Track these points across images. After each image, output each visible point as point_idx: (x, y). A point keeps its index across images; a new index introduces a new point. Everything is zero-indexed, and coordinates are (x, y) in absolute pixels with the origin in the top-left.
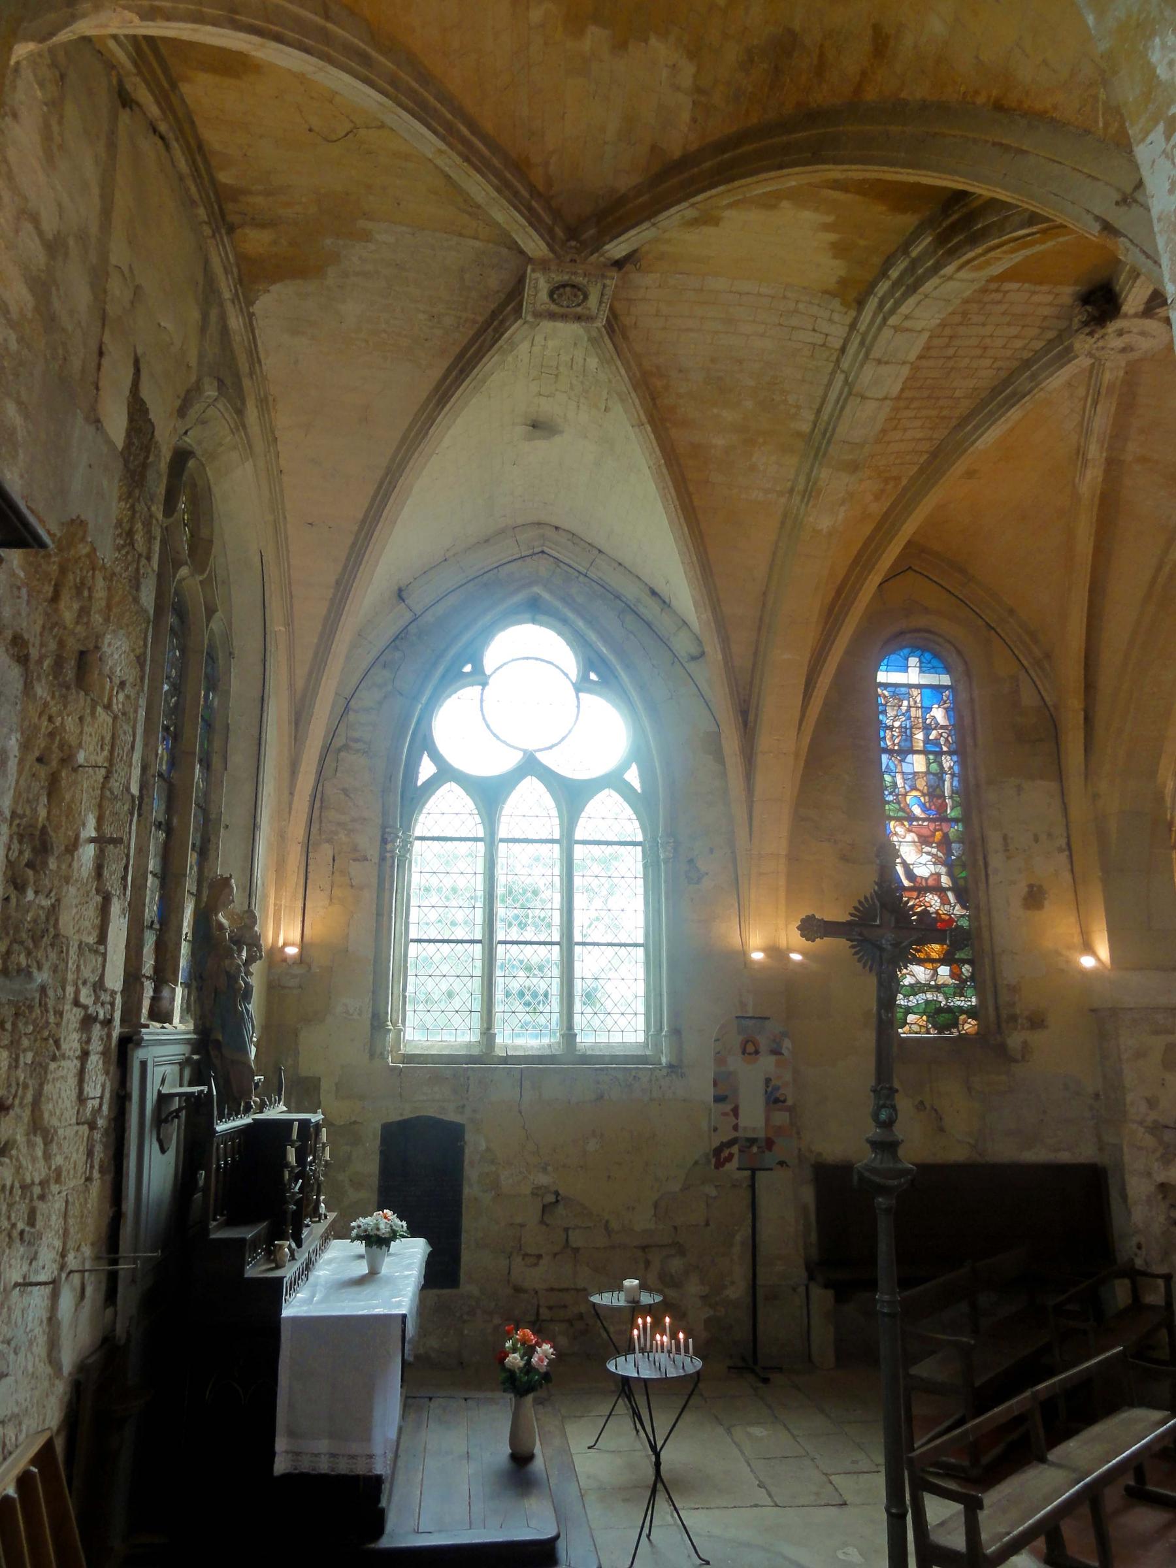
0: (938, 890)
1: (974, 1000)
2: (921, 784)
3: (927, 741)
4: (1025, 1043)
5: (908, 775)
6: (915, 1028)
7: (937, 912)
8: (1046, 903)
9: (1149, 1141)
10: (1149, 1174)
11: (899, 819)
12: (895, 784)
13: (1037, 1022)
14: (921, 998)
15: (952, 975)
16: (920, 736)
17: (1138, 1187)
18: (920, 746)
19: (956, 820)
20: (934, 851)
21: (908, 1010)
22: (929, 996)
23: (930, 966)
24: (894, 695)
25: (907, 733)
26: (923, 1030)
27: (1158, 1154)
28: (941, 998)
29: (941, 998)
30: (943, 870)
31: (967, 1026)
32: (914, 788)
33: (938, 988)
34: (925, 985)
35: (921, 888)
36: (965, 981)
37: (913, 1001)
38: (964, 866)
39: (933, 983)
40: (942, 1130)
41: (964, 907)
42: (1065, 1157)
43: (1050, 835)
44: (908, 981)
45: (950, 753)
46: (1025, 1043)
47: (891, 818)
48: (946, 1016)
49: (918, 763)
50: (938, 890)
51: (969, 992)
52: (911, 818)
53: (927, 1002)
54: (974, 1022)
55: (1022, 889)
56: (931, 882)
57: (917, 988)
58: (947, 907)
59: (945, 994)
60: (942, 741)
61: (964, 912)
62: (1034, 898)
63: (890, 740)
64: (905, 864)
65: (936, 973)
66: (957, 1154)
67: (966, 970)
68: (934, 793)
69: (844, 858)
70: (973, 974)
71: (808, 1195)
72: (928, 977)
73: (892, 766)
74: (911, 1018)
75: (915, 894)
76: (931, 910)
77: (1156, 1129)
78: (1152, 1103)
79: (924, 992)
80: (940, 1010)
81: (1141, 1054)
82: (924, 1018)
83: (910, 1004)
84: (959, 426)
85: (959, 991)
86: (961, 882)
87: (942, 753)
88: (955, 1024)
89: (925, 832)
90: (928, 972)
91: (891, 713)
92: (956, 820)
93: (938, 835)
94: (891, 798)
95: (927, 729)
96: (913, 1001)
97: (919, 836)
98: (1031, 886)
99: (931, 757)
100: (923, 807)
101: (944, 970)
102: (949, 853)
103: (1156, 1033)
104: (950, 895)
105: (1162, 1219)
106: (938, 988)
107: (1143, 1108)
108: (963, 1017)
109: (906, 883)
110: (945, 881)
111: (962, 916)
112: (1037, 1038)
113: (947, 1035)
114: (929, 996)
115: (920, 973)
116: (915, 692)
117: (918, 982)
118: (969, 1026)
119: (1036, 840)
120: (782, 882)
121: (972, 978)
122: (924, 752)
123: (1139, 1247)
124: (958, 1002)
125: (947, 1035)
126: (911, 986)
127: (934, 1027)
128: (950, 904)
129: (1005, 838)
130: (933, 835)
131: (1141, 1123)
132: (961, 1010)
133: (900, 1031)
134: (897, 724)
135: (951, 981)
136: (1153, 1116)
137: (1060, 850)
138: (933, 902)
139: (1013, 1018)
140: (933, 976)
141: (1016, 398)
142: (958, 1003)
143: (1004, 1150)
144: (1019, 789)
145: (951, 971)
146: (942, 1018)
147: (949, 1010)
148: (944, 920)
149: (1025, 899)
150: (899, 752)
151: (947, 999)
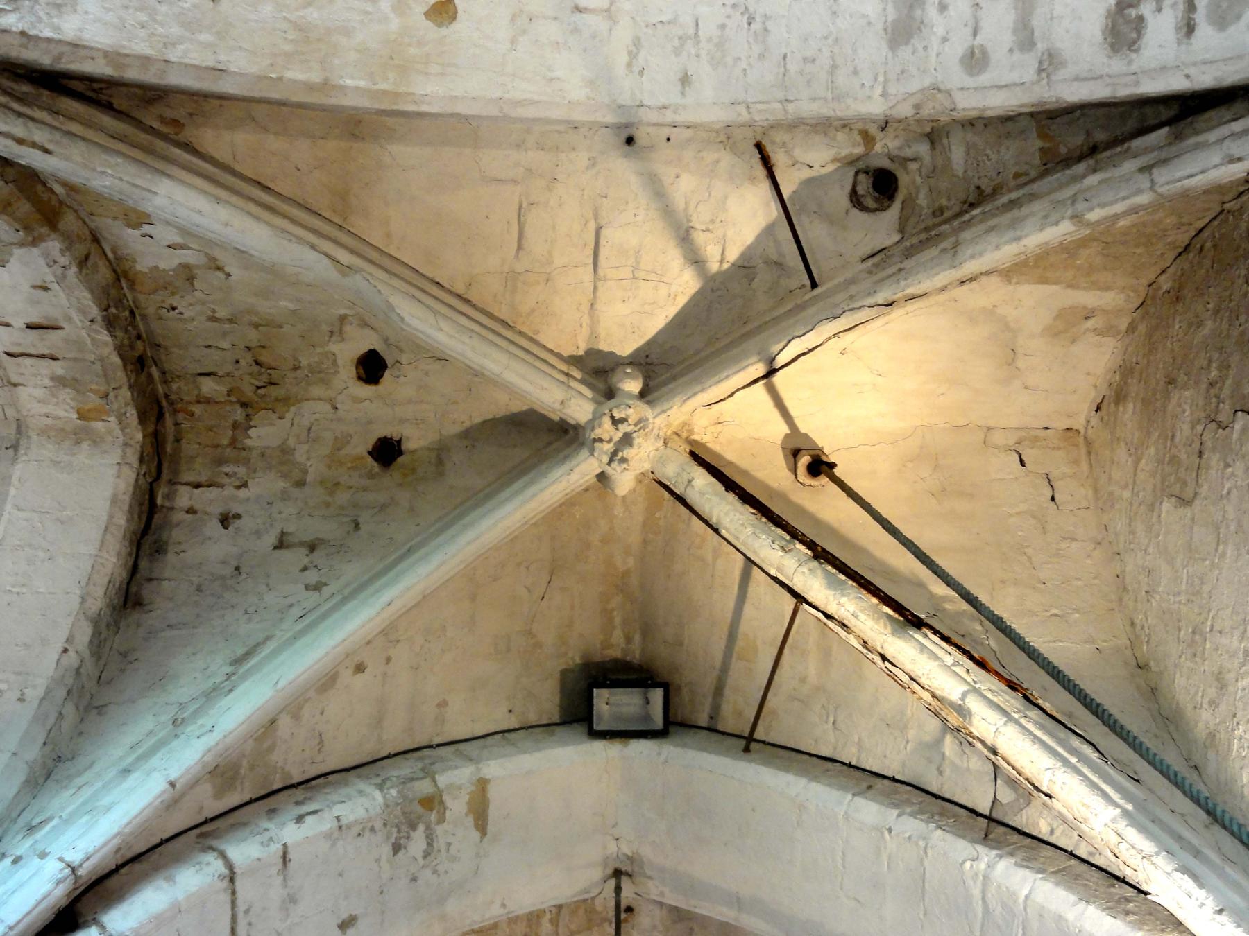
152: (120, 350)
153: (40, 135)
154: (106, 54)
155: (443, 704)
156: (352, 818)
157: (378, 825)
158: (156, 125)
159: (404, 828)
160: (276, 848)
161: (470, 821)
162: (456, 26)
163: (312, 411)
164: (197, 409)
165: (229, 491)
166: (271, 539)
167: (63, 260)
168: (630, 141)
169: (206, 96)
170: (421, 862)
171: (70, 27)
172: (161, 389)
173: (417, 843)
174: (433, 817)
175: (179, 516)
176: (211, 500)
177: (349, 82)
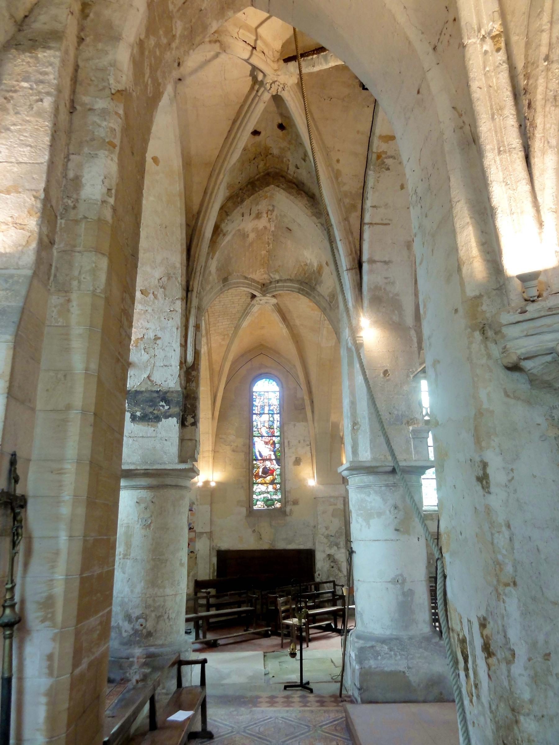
0: (270, 460)
2: (266, 425)
3: (269, 410)
4: (291, 510)
5: (261, 422)
6: (260, 506)
8: (301, 463)
9: (325, 541)
10: (324, 551)
11: (258, 437)
12: (257, 425)
13: (295, 503)
14: (262, 496)
15: (273, 488)
16: (266, 409)
17: (320, 557)
18: (266, 411)
19: (278, 436)
20: (270, 447)
21: (257, 500)
22: (265, 495)
23: (265, 485)
24: (260, 395)
25: (263, 408)
27: (328, 545)
28: (269, 496)
30: (272, 453)
32: (264, 426)
33: (268, 493)
35: (264, 460)
37: (259, 497)
38: (279, 451)
40: (261, 539)
41: (279, 465)
42: (302, 547)
43: (304, 440)
44: (258, 491)
45: (277, 414)
46: (291, 510)
47: (255, 436)
49: (265, 418)
50: (270, 460)
51: (279, 494)
52: (262, 436)
55: (293, 459)
56: (268, 457)
57: (261, 493)
60: (275, 410)
62: (298, 462)
63: (256, 410)
64: (259, 452)
66: (266, 547)
67: (278, 486)
68: (271, 428)
69: (234, 451)
71: (215, 560)
73: (257, 419)
74: (258, 503)
75: (262, 461)
77: (327, 537)
78: (327, 528)
80: (268, 500)
81: (324, 512)
84: (239, 320)
86: (278, 457)
87: (274, 414)
89: (267, 440)
91: (257, 400)
92: (278, 436)
93: (271, 441)
94: (256, 430)
95: (269, 406)
96: (259, 497)
97: (265, 442)
98: (296, 458)
99: (270, 415)
100: (268, 433)
102: (275, 447)
103: (331, 505)
104: (274, 462)
105: (328, 566)
106: (268, 493)
107: (324, 530)
109: (259, 458)
110: (273, 457)
112: (295, 508)
113: (270, 508)
115: (263, 488)
116: (266, 393)
118: (278, 505)
119: (299, 442)
120: (211, 460)
121: (280, 489)
122: (269, 414)
123: (319, 575)
124: (275, 497)
125: (270, 508)
126: (259, 492)
127: (266, 505)
129: (289, 442)
130: (269, 442)
131: (322, 535)
132: (276, 500)
134: (259, 405)
136: (327, 532)
137: (307, 445)
139: (288, 502)
141: (248, 313)
143: (281, 545)
144: (295, 425)
146: (269, 502)
147: (272, 500)
149: (294, 462)
150: (259, 414)
152: (249, 197)
153: (199, 269)
154: (182, 256)
155: (358, 132)
156: (372, 184)
157: (378, 175)
158: (194, 222)
159: (383, 166)
160: (370, 209)
161: (390, 142)
162: (158, 157)
163: (270, 143)
164: (267, 165)
165: (290, 163)
166: (303, 162)
167: (226, 221)
168: (180, 80)
169: (186, 210)
170: (396, 160)
171: (178, 265)
172: (262, 174)
173: (389, 162)
174: (384, 156)
175: (295, 175)
176: (292, 169)
177: (178, 189)
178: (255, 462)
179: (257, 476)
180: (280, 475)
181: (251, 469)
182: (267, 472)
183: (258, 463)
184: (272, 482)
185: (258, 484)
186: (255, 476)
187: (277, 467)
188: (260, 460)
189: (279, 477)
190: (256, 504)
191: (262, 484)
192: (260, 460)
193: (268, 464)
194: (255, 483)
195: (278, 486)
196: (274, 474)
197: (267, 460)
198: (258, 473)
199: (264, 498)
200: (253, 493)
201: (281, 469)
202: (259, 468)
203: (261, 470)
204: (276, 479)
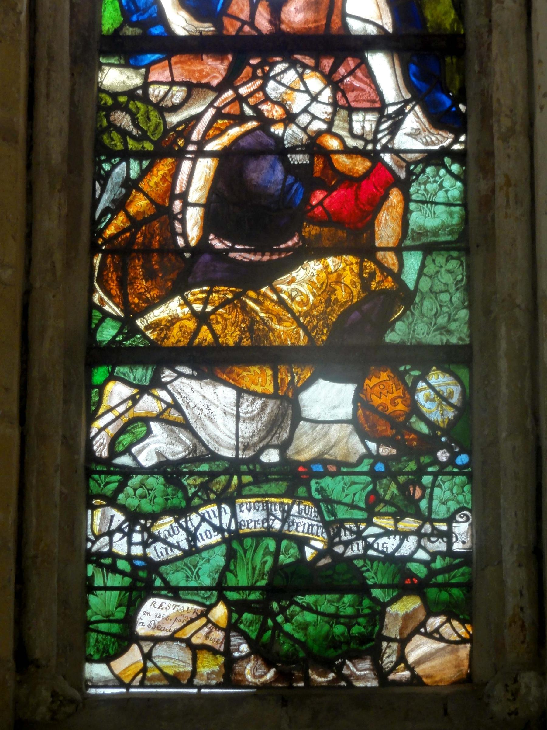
1: (462, 529)
6: (172, 659)
7: (313, 146)
14: (209, 523)
15: (366, 419)
23: (259, 378)
26: (209, 666)
28: (305, 522)
29: (305, 522)
31: (419, 648)
33: (295, 478)
34: (234, 466)
36: (429, 444)
39: (272, 456)
41: (439, 119)
44: (157, 446)
48: (326, 603)
51: (447, 494)
53: (234, 541)
54: (454, 629)
57: (196, 479)
58: (365, 122)
59: (324, 503)
61: (444, 139)
65: (287, 411)
70: (465, 409)
72: (248, 429)
74: (155, 614)
75: (214, 69)
76: (292, 134)
79: (227, 498)
80: (290, 581)
82: (220, 612)
83: (158, 551)
85: (397, 488)
88: (368, 645)
90: (250, 407)
101: (328, 400)
106: (295, 478)
108: (410, 604)
111: (434, 158)
114: (250, 515)
115: (218, 412)
117: (202, 454)
118: (433, 652)
121: (462, 430)
124: (392, 540)
126: (169, 471)
127: (262, 651)
128: (379, 107)
132: (404, 579)
133: (97, 671)
135: (356, 446)
138: (298, 102)
140: (273, 425)
142: (389, 544)
145: (360, 400)
146: (306, 618)
147: (337, 575)
148: (346, 179)
151: (333, 527)
178: (115, 77)
179: (151, 254)
180: (469, 241)
181: (54, 145)
182: (278, 203)
183: (163, 81)
184: (354, 342)
185: (159, 357)
186: (122, 252)
187: (414, 134)
188: (194, 46)
189: (449, 272)
190: (127, 637)
191: (210, 361)
192: (194, 46)
193: (299, 96)
194: (115, 356)
195: (436, 395)
196: (386, 229)
197: (287, 45)
198: (164, 213)
199: (234, 541)
200: (93, 476)
201: (474, 165)
202: (171, 147)
203: (198, 177)
204: (405, 297)
